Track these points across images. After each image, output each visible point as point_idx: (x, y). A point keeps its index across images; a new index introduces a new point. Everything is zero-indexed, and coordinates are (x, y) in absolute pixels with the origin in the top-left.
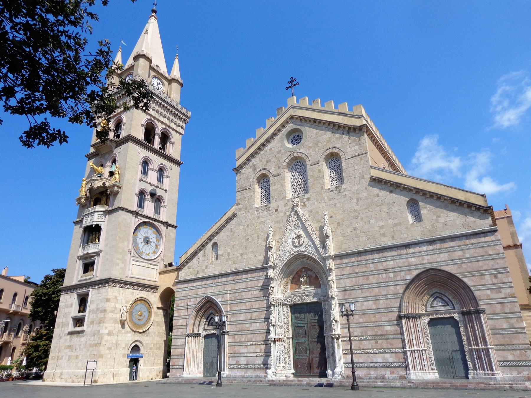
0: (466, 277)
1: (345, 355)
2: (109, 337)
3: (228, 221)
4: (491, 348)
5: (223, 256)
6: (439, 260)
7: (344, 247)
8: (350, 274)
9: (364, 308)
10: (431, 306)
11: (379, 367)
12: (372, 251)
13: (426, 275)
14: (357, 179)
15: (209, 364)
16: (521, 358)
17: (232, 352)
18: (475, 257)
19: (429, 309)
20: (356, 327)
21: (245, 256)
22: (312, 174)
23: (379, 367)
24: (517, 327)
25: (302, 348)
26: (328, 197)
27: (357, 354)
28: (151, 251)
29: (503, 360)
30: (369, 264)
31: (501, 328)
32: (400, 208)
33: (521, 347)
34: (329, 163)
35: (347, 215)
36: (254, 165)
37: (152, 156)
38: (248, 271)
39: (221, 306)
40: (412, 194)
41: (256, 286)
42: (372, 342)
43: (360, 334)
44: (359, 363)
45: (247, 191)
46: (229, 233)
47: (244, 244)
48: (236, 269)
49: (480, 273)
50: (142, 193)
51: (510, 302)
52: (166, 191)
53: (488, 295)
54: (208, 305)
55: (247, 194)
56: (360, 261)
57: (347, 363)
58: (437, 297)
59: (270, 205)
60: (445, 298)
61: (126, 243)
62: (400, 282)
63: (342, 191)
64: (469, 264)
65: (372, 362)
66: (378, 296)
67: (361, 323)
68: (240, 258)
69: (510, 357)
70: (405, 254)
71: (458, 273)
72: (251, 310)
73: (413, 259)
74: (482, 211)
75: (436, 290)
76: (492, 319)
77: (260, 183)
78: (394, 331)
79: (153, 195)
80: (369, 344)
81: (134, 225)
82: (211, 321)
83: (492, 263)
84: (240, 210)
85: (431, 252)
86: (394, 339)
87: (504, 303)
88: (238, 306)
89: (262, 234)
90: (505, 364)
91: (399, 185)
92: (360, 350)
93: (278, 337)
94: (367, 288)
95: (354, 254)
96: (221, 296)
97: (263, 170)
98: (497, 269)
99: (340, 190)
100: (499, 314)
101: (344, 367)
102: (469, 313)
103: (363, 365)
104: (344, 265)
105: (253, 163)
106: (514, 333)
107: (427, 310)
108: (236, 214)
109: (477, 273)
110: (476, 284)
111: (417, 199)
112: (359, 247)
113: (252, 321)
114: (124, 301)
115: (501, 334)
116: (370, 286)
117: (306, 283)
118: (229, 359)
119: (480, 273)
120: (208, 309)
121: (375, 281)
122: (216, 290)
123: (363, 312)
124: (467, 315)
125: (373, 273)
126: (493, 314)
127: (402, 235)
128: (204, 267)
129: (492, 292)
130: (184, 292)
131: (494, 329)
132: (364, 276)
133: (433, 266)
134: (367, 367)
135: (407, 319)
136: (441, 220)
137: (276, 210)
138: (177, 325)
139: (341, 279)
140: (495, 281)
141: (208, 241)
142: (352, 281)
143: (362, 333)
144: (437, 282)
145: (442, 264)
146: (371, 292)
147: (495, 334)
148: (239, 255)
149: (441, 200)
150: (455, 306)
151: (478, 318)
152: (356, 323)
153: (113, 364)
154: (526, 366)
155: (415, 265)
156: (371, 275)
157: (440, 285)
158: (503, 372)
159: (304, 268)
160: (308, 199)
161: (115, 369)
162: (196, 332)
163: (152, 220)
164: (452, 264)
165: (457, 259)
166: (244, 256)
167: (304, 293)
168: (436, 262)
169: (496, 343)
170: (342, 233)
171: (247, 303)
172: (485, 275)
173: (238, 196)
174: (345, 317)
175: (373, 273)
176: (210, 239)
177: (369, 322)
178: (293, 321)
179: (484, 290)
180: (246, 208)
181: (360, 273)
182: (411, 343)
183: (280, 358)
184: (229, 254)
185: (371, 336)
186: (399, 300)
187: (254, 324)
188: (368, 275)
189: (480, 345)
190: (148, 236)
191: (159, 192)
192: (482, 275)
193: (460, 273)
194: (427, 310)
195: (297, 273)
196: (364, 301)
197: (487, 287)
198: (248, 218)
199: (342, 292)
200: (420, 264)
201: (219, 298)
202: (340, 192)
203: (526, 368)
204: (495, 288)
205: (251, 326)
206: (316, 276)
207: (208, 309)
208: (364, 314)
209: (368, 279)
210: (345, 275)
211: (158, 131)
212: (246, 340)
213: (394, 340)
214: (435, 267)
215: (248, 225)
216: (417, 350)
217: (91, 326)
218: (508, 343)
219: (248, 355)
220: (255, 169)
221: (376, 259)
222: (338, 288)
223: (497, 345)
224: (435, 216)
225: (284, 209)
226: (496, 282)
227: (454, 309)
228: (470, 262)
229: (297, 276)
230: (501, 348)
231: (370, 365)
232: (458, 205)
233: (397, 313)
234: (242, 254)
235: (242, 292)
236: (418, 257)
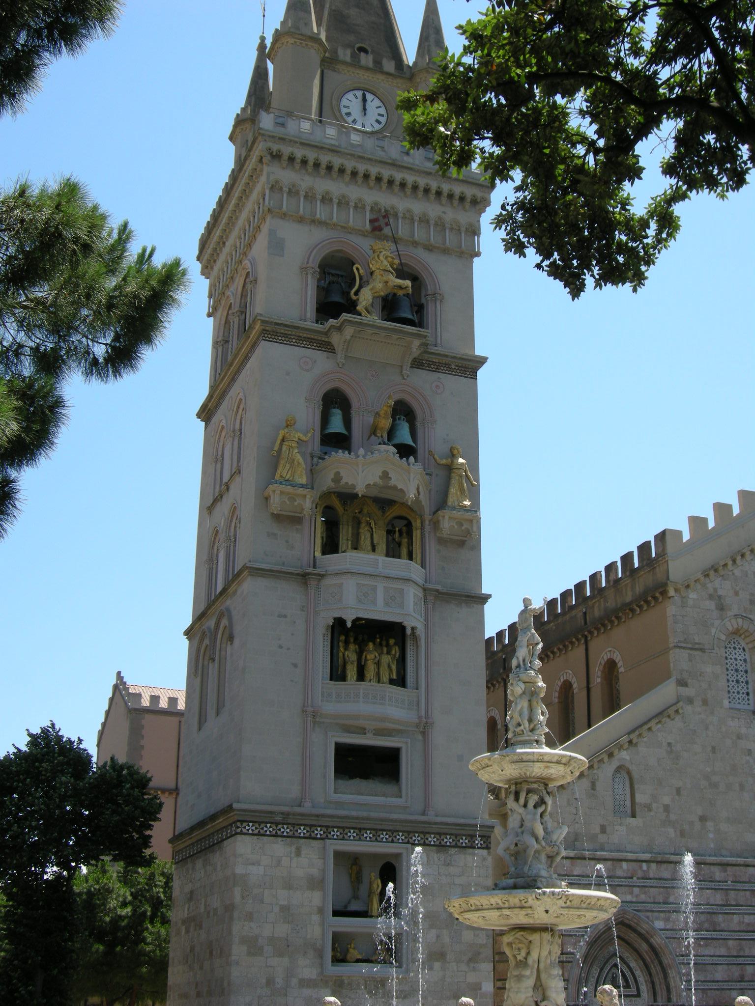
5: (650, 810)
36: (720, 597)
41: (749, 903)
72: (741, 960)
96: (662, 915)
97: (743, 617)
105: (715, 590)
122: (643, 897)
128: (597, 830)
166: (710, 825)
171: (730, 942)
180: (705, 702)
184: (667, 808)
201: (657, 919)
217: (437, 965)
220: (721, 608)
234: (703, 819)
235: (714, 913)
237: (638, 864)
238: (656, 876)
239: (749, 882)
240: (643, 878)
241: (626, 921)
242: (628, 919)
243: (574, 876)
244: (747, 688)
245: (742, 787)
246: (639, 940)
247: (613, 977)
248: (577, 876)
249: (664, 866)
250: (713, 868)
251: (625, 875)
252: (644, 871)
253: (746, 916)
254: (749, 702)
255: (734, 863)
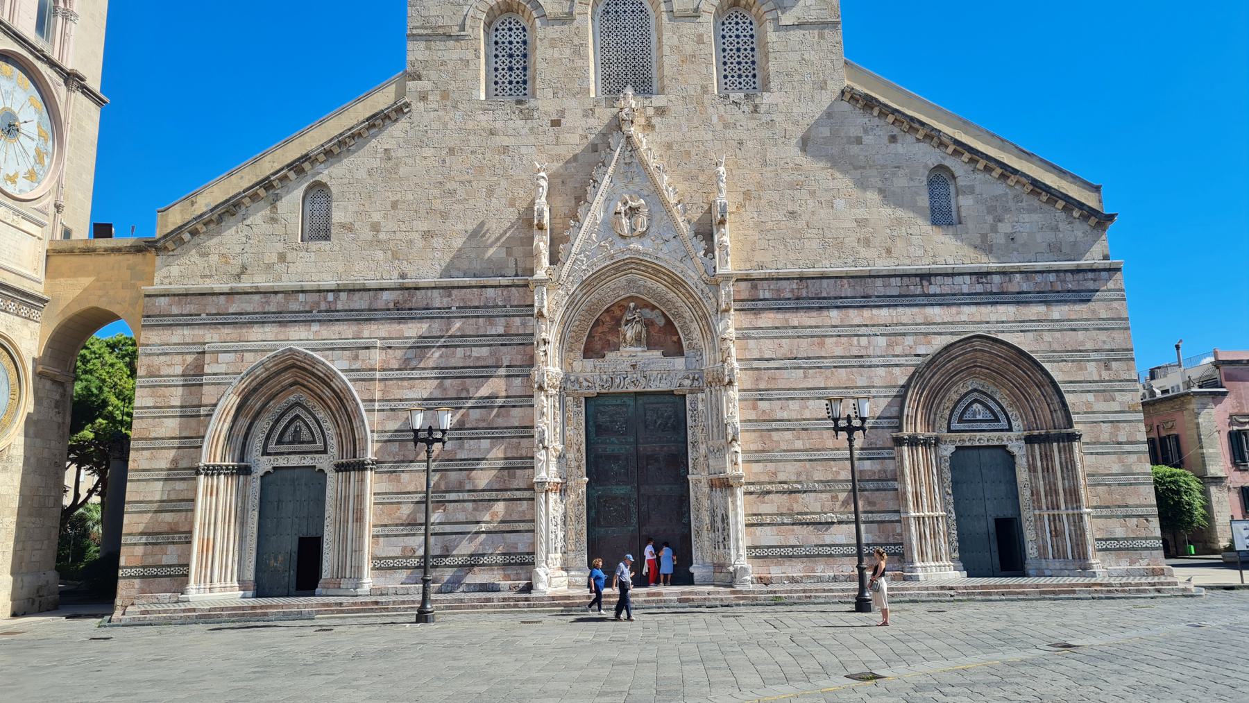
0: (1048, 362)
1: (751, 529)
3: (378, 121)
4: (1089, 514)
5: (351, 230)
6: (994, 318)
7: (759, 257)
8: (777, 328)
9: (807, 415)
10: (961, 421)
11: (838, 556)
12: (837, 277)
13: (962, 349)
14: (808, 87)
15: (280, 558)
16: (1138, 534)
17: (386, 522)
18: (1072, 320)
19: (955, 426)
20: (786, 461)
21: (440, 240)
22: (675, 41)
23: (838, 556)
24: (1137, 471)
25: (616, 510)
26: (720, 117)
27: (783, 524)
28: (23, 169)
29: (1105, 537)
31: (1107, 472)
32: (912, 183)
33: (1140, 511)
34: (723, 24)
35: (772, 175)
38: (454, 288)
39: (350, 384)
40: (942, 154)
42: (824, 496)
43: (794, 478)
44: (787, 547)
45: (451, 43)
46: (376, 163)
47: (438, 204)
48: (403, 276)
49: (1078, 356)
51: (1130, 421)
53: (1088, 404)
54: (287, 378)
55: (451, 52)
56: (804, 299)
57: (756, 547)
58: (976, 401)
59: (532, 103)
60: (992, 404)
62: (902, 360)
63: (763, 109)
64: (1058, 334)
65: (821, 543)
66: (846, 388)
67: (798, 451)
68: (420, 243)
69: (1119, 532)
70: (919, 295)
71: (1032, 352)
73: (937, 310)
74: (1093, 221)
75: (975, 386)
76: (1092, 453)
77: (493, 27)
78: (879, 471)
80: (816, 500)
82: (292, 429)
83: (1103, 336)
84: (423, 97)
85: (977, 299)
86: (878, 490)
87: (1118, 422)
88: (411, 388)
89: (503, 182)
90: (1112, 546)
91: (916, 125)
92: (790, 515)
94: (818, 367)
95: (788, 279)
98: (1112, 350)
99: (756, 106)
100: (1107, 443)
101: (748, 558)
102: (1045, 439)
103: (796, 552)
104: (760, 304)
106: (1131, 484)
107: (952, 428)
108: (407, 105)
109: (1072, 356)
110: (1067, 379)
111: (953, 169)
112: (801, 263)
113: (465, 434)
115: (1106, 485)
116: (827, 362)
117: (638, 340)
118: (377, 543)
119: (1078, 356)
120: (284, 389)
121: (838, 351)
123: (804, 424)
124: (1039, 444)
125: (836, 331)
126: (1094, 443)
127: (911, 250)
128: (274, 258)
129: (1097, 400)
130: (186, 331)
131: (1093, 475)
132: (812, 336)
133: (981, 330)
134: (806, 556)
135: (912, 445)
136: (1005, 228)
137: (556, 123)
138: (153, 435)
139: (750, 338)
140: (1105, 375)
141: (292, 175)
142: (780, 346)
143: (799, 474)
144: (979, 367)
145: (1000, 327)
146: (827, 378)
147: (1095, 485)
148: (417, 236)
149: (1009, 182)
150: (1013, 424)
151: (1065, 451)
152: (785, 451)
154: (1146, 548)
155: (939, 324)
156: (832, 336)
157: (985, 375)
158: (1103, 561)
159: (632, 298)
160: (661, 111)
163: (31, 53)
164: (1022, 331)
165: (1033, 321)
166: (438, 242)
167: (634, 366)
168: (988, 322)
169: (1095, 504)
170: (756, 219)
172: (1088, 361)
173: (416, 52)
174: (843, 435)
175: (836, 331)
176: (297, 166)
177: (818, 450)
178: (593, 436)
179: (1082, 392)
180: (445, 95)
181: (803, 327)
182: (918, 505)
183: (556, 537)
184: (376, 228)
185: (822, 481)
187: (472, 442)
188: (823, 336)
189: (1063, 507)
190: (15, 109)
192: (1081, 361)
193: (1037, 352)
194: (952, 428)
195: (607, 310)
196: (808, 399)
197: (1087, 387)
198: (451, 125)
199: (751, 372)
200: (952, 323)
202: (756, 111)
203: (1145, 553)
204: (1104, 391)
205: (461, 447)
206: (669, 323)
207: (284, 389)
208: (806, 429)
209: (822, 345)
210: (761, 328)
212: (443, 487)
213: (877, 493)
214: (984, 332)
215: (452, 151)
218: (1118, 503)
219: (448, 529)
221: (846, 298)
222: (741, 360)
223: (1095, 507)
224: (991, 217)
225: (583, 123)
226: (1107, 378)
227: (1010, 429)
228: (1060, 330)
229: (608, 319)
230: (1105, 512)
231: (815, 551)
232: (1044, 198)
234: (427, 235)
236: (948, 305)
237: (322, 294)
238: (346, 308)
239: (486, 307)
240: (326, 311)
241: (298, 363)
242: (297, 360)
243: (229, 314)
244: (525, 75)
245: (491, 192)
246: (321, 386)
247: (295, 431)
248: (233, 314)
249: (357, 295)
250: (429, 292)
251: (301, 309)
252: (330, 302)
253: (473, 349)
254: (526, 92)
255: (461, 284)
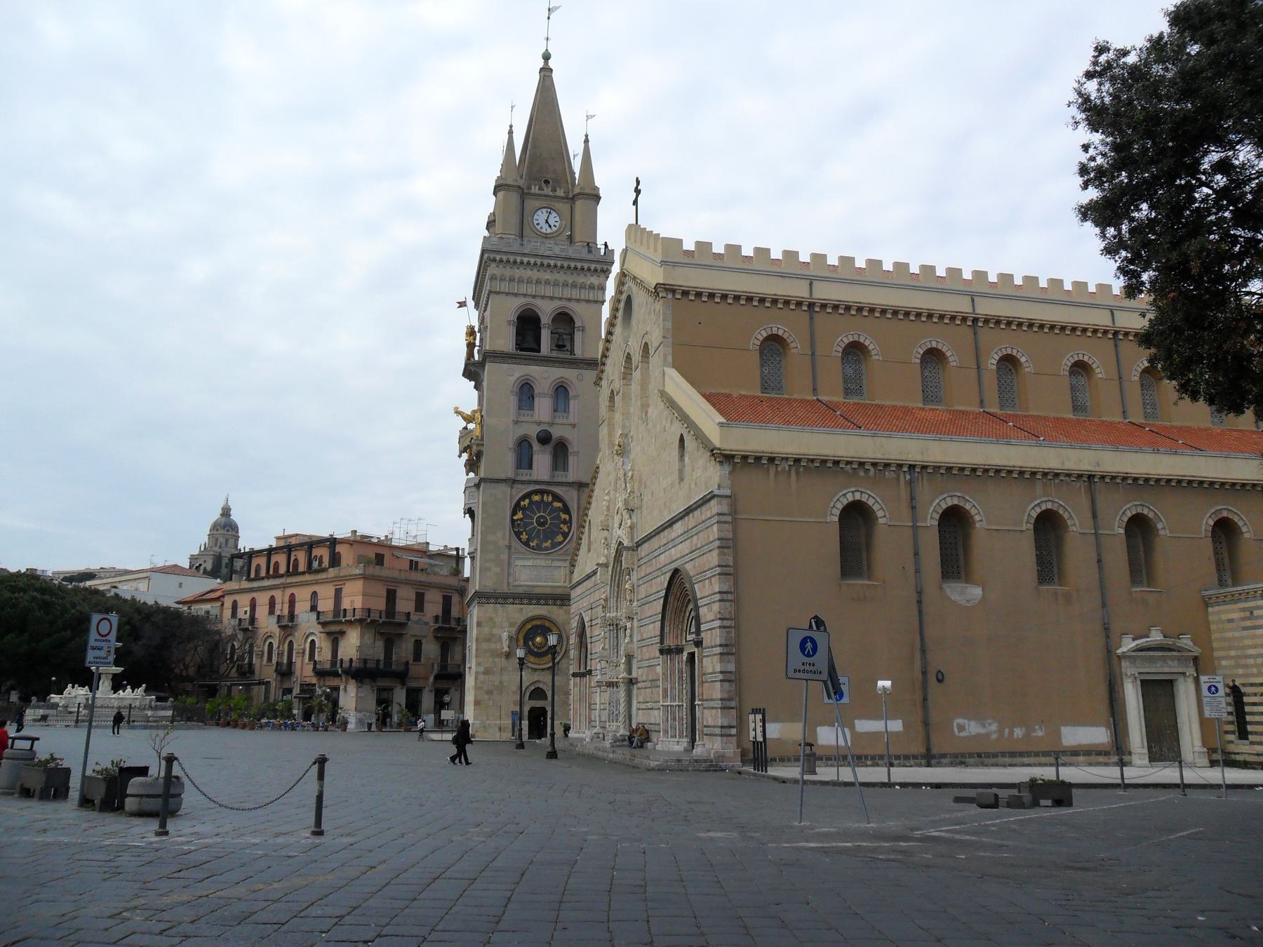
2: (487, 677)
30: (652, 559)
37: (535, 371)
50: (523, 445)
52: (574, 426)
61: (500, 534)
79: (544, 439)
81: (511, 504)
93: (610, 680)
107: (688, 640)
114: (506, 624)
153: (499, 714)
161: (502, 722)
162: (582, 670)
183: (613, 713)
186: (658, 624)
191: (556, 432)
211: (545, 319)
216: (671, 706)
233: (659, 645)
